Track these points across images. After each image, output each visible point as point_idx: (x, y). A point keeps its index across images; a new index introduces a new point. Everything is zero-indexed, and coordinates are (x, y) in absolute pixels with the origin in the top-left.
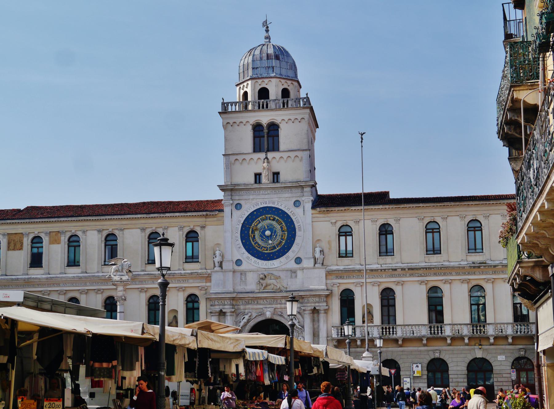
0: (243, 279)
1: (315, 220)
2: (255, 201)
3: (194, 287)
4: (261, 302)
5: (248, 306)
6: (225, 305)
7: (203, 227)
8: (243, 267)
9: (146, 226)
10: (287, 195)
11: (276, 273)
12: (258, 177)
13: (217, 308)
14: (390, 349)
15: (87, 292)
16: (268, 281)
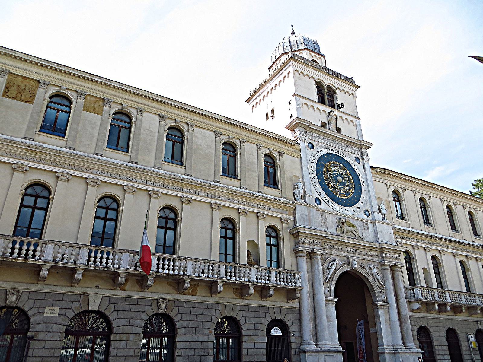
0: (324, 220)
1: (375, 178)
2: (324, 146)
3: (274, 216)
4: (344, 248)
5: (334, 252)
6: (314, 245)
7: (281, 154)
8: (322, 206)
9: (222, 131)
10: (349, 150)
11: (351, 221)
12: (324, 125)
13: (305, 247)
14: (450, 317)
15: (133, 191)
16: (345, 227)
